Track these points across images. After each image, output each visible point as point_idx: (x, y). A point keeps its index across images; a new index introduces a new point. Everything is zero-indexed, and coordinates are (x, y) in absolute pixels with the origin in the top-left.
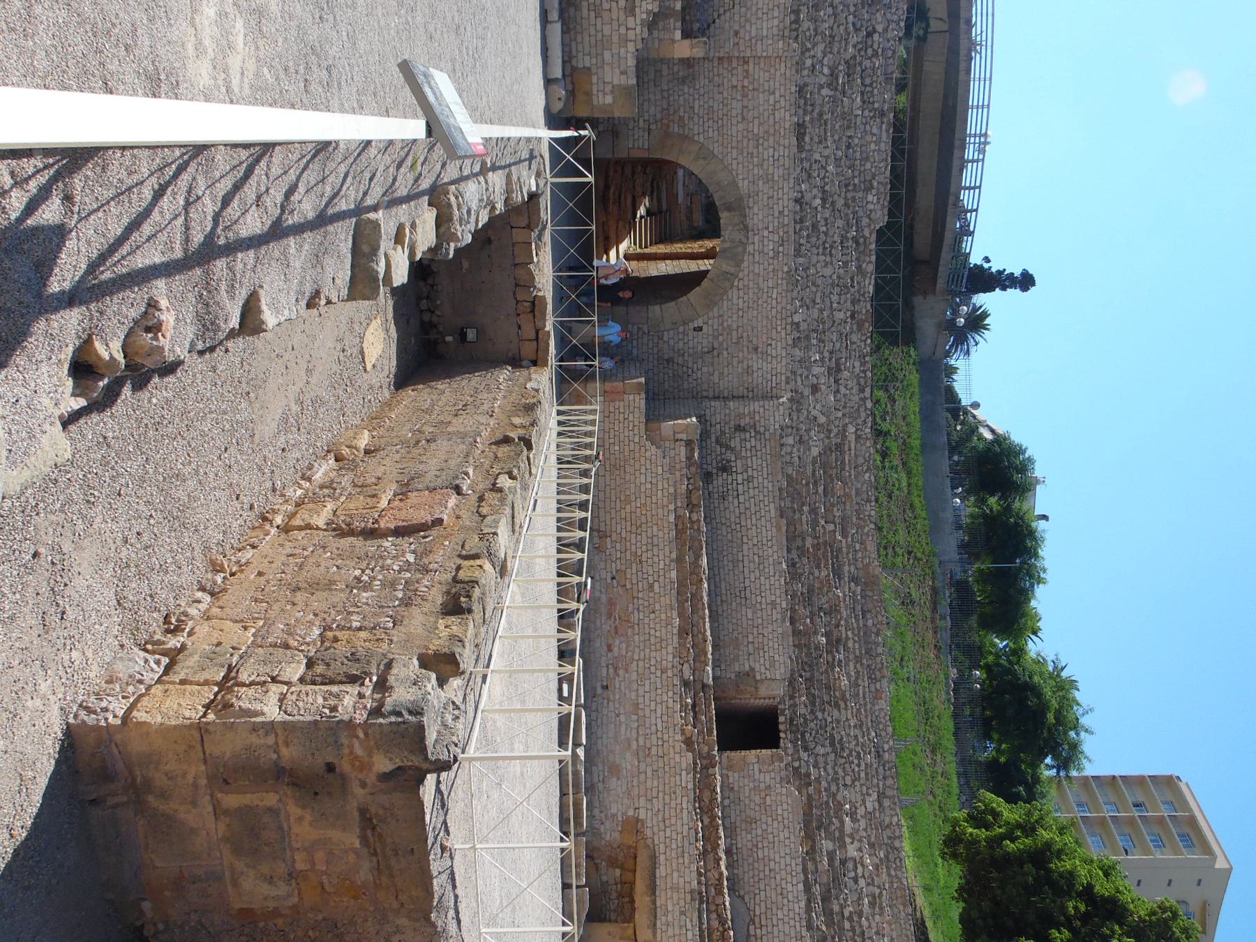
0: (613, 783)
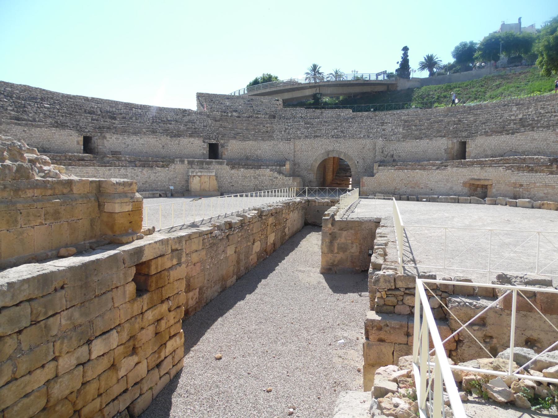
0: (454, 189)
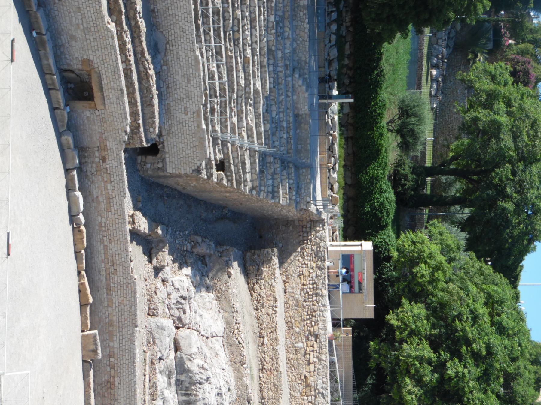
0: (73, 43)
